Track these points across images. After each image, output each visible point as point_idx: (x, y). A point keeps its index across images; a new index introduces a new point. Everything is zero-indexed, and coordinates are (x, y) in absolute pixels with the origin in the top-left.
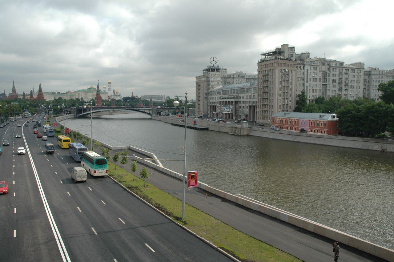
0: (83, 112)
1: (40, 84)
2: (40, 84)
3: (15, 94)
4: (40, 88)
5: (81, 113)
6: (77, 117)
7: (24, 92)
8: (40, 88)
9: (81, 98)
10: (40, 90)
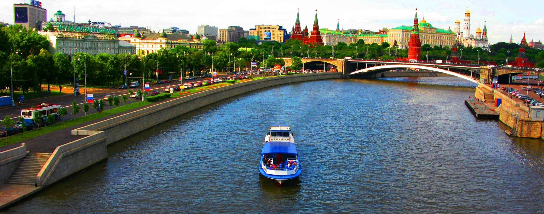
0: (359, 69)
1: (316, 14)
2: (316, 14)
3: (299, 33)
4: (316, 23)
5: (356, 71)
6: (348, 77)
9: (394, 41)
10: (316, 28)
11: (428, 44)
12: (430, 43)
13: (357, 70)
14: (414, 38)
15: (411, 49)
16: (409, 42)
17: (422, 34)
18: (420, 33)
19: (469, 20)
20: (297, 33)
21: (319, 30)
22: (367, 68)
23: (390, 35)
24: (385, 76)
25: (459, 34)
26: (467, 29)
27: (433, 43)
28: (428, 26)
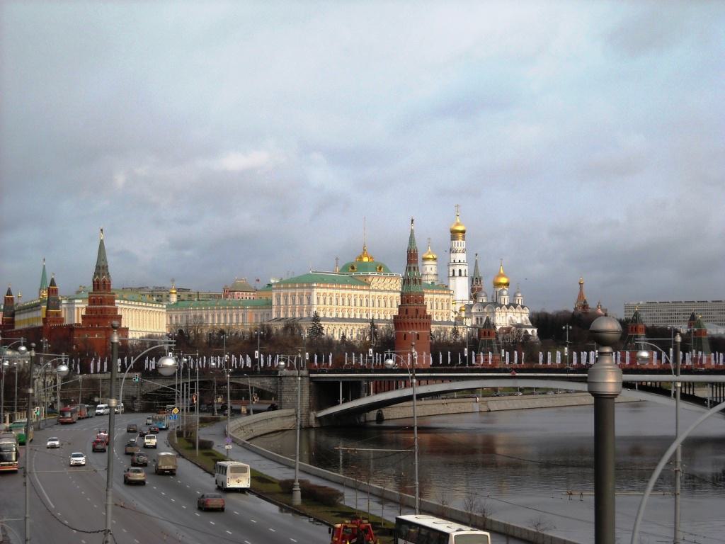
1: (102, 242)
2: (102, 242)
4: (101, 268)
5: (338, 403)
7: (9, 293)
8: (98, 267)
17: (367, 293)
21: (112, 292)
23: (278, 300)
24: (385, 418)
26: (460, 275)
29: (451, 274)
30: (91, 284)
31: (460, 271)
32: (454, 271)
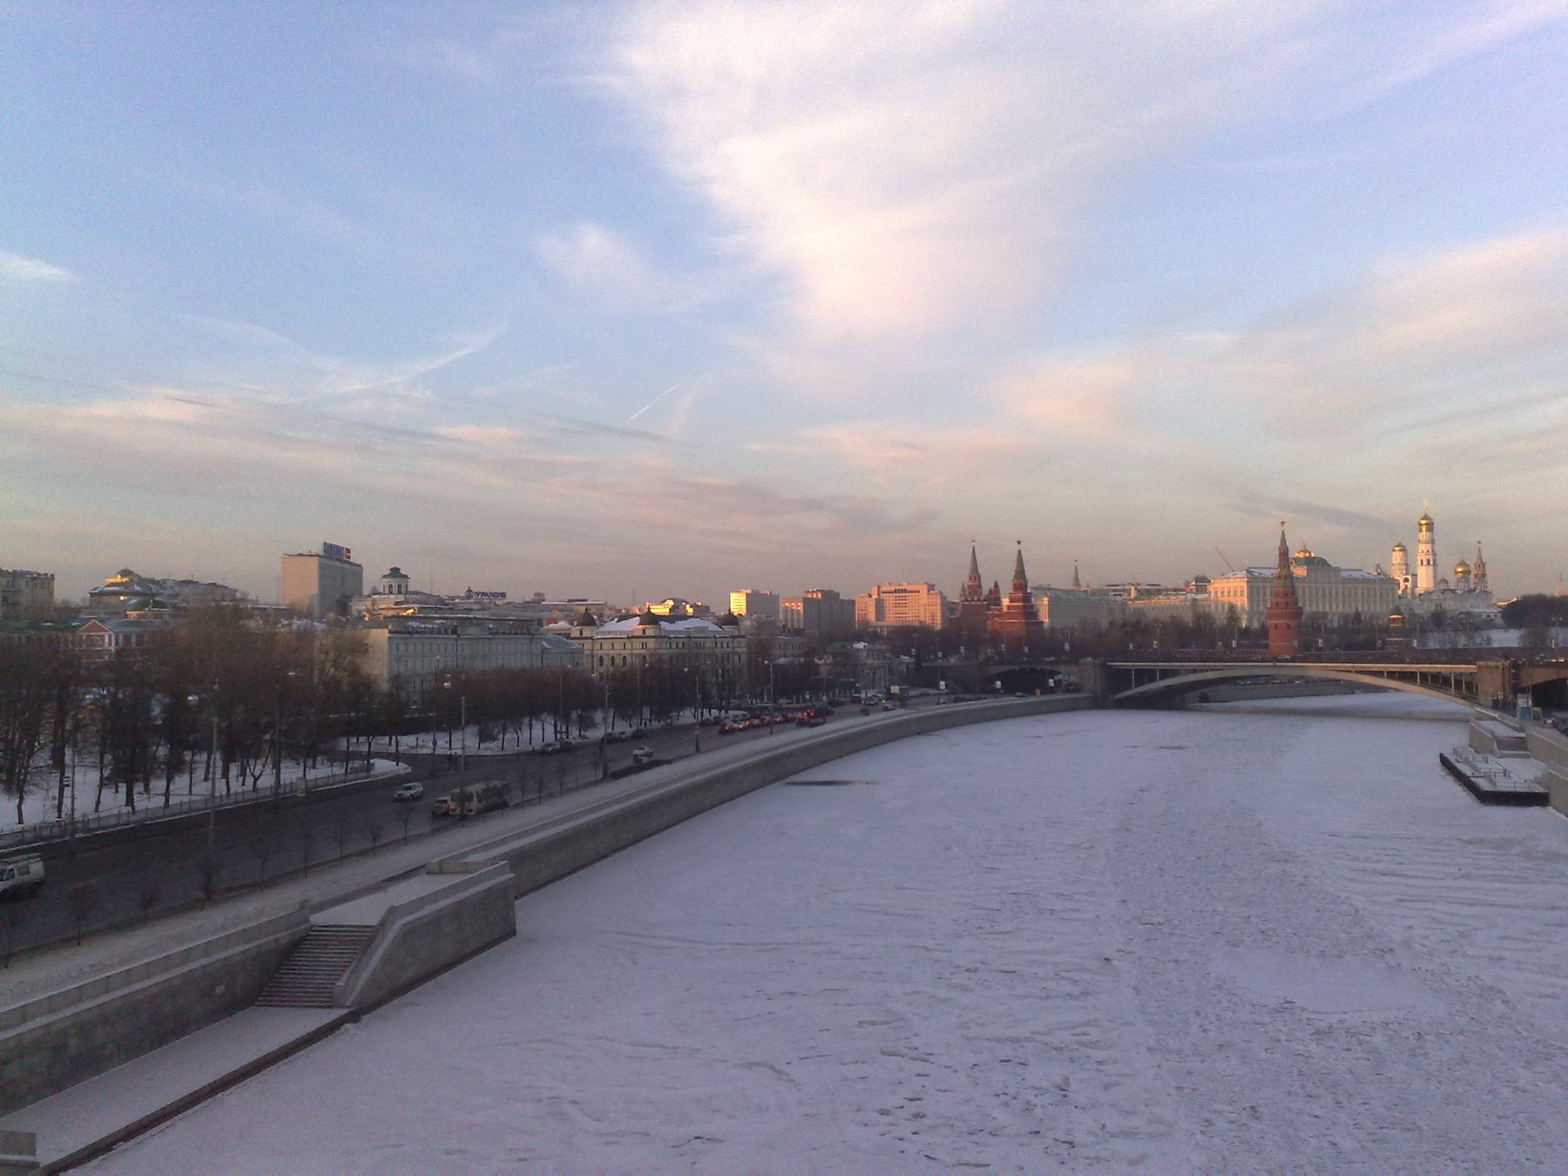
0: (1140, 683)
1: (1020, 551)
2: (1020, 551)
3: (979, 600)
4: (1020, 573)
5: (1129, 688)
11: (1321, 609)
12: (1327, 608)
13: (1133, 686)
14: (1281, 600)
15: (1276, 627)
16: (1270, 609)
18: (1296, 584)
19: (1432, 542)
20: (973, 600)
22: (1161, 679)
25: (1406, 580)
26: (1429, 564)
27: (1334, 609)
28: (1316, 564)
29: (1420, 563)
30: (1012, 587)
31: (1429, 560)
32: (1422, 561)
